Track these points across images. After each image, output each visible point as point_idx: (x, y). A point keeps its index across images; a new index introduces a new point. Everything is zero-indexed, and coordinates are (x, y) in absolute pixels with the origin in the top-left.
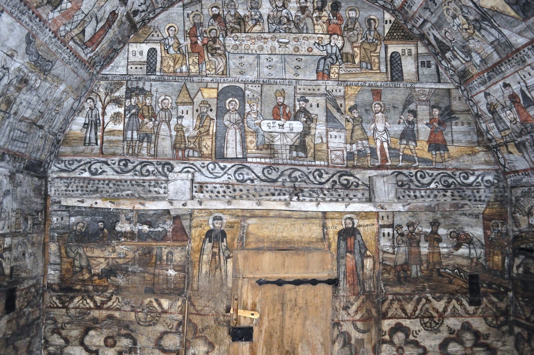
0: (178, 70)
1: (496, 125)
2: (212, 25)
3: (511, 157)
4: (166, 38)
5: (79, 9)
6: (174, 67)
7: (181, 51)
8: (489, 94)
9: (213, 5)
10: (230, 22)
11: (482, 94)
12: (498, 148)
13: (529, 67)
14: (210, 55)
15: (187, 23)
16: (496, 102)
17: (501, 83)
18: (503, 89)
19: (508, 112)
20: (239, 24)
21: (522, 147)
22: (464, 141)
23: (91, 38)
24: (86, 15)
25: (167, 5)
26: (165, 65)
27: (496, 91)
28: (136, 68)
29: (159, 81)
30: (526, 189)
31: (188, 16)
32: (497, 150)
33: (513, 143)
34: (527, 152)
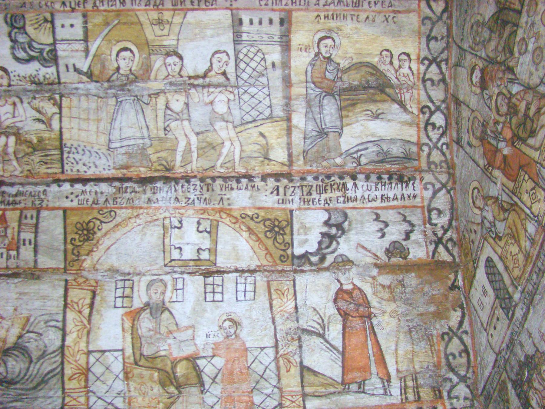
0: (528, 244)
2: (490, 97)
4: (482, 221)
5: (246, 350)
6: (520, 249)
7: (505, 205)
9: (469, 77)
10: (496, 48)
14: (531, 141)
15: (477, 157)
20: (505, 23)
23: (343, 367)
24: (276, 346)
25: (444, 178)
26: (511, 267)
28: (495, 328)
29: (528, 309)
31: (470, 145)
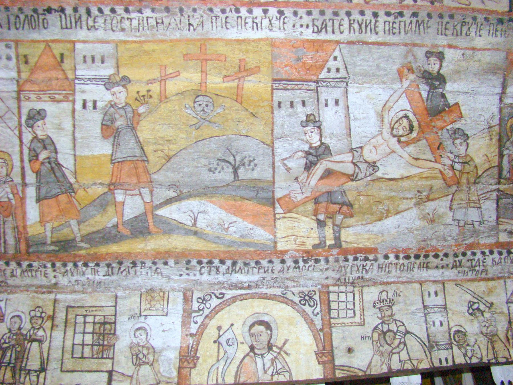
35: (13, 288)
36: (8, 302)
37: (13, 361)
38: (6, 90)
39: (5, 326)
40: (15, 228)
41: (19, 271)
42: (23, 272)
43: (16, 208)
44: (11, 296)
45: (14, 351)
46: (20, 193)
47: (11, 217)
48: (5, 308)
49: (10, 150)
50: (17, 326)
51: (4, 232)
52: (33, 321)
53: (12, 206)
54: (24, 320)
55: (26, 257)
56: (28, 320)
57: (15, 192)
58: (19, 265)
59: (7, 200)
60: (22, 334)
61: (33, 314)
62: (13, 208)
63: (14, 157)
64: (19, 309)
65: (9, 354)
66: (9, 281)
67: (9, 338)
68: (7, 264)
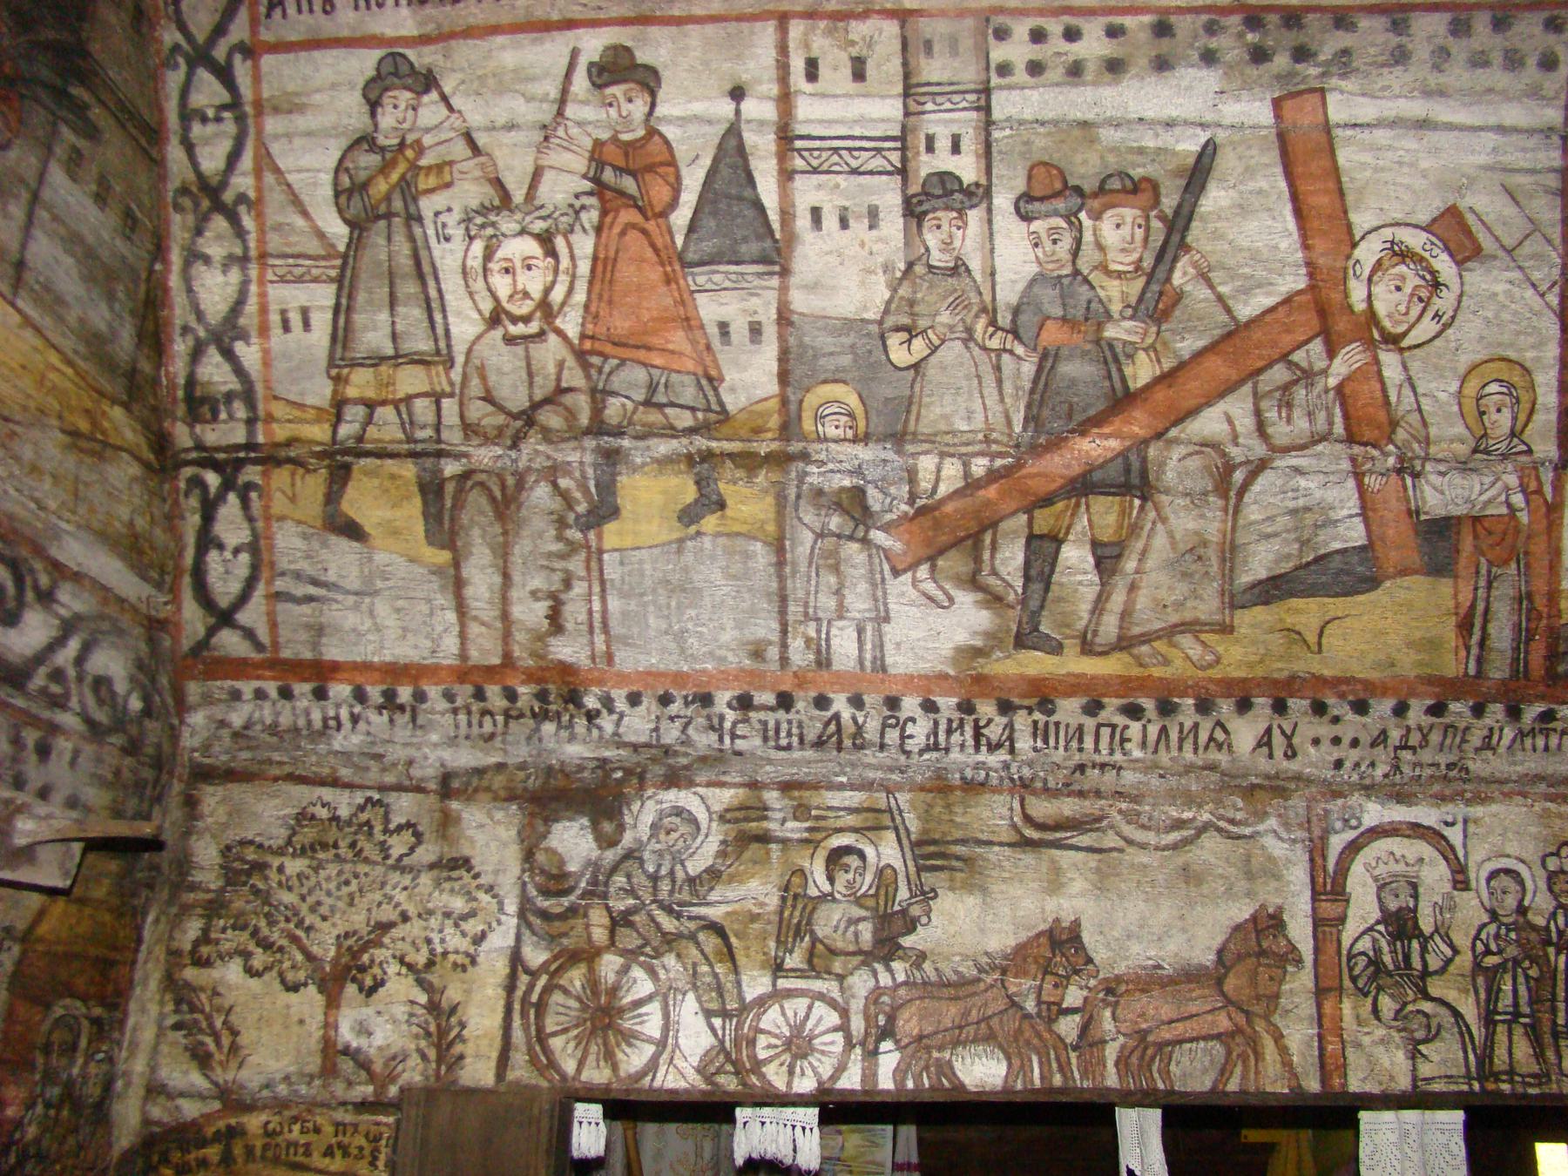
1: (343, 311)
3: (341, 559)
8: (427, 82)
11: (365, 62)
12: (251, 474)
13: (891, 28)
16: (460, 149)
17: (593, 44)
18: (580, 83)
19: (520, 248)
21: (477, 513)
22: (72, 317)
27: (523, 76)
30: (345, 804)
32: (227, 486)
33: (408, 470)
34: (503, 553)
35: (1483, 787)
36: (1471, 828)
37: (1525, 1009)
38: (1526, 165)
39: (1475, 902)
40: (1524, 599)
41: (1508, 734)
42: (1522, 734)
43: (1529, 537)
44: (1478, 811)
45: (1521, 979)
46: (1548, 490)
47: (1513, 565)
48: (1465, 846)
49: (1529, 354)
50: (1511, 902)
51: (1487, 611)
52: (1556, 888)
53: (1517, 531)
54: (1529, 885)
55: (1541, 688)
56: (1542, 885)
57: (1533, 486)
58: (1514, 713)
59: (1504, 510)
60: (1534, 928)
61: (1552, 863)
62: (1522, 537)
63: (1539, 378)
64: (1509, 850)
65: (1507, 987)
66: (1471, 765)
67: (1497, 936)
68: (1478, 711)
